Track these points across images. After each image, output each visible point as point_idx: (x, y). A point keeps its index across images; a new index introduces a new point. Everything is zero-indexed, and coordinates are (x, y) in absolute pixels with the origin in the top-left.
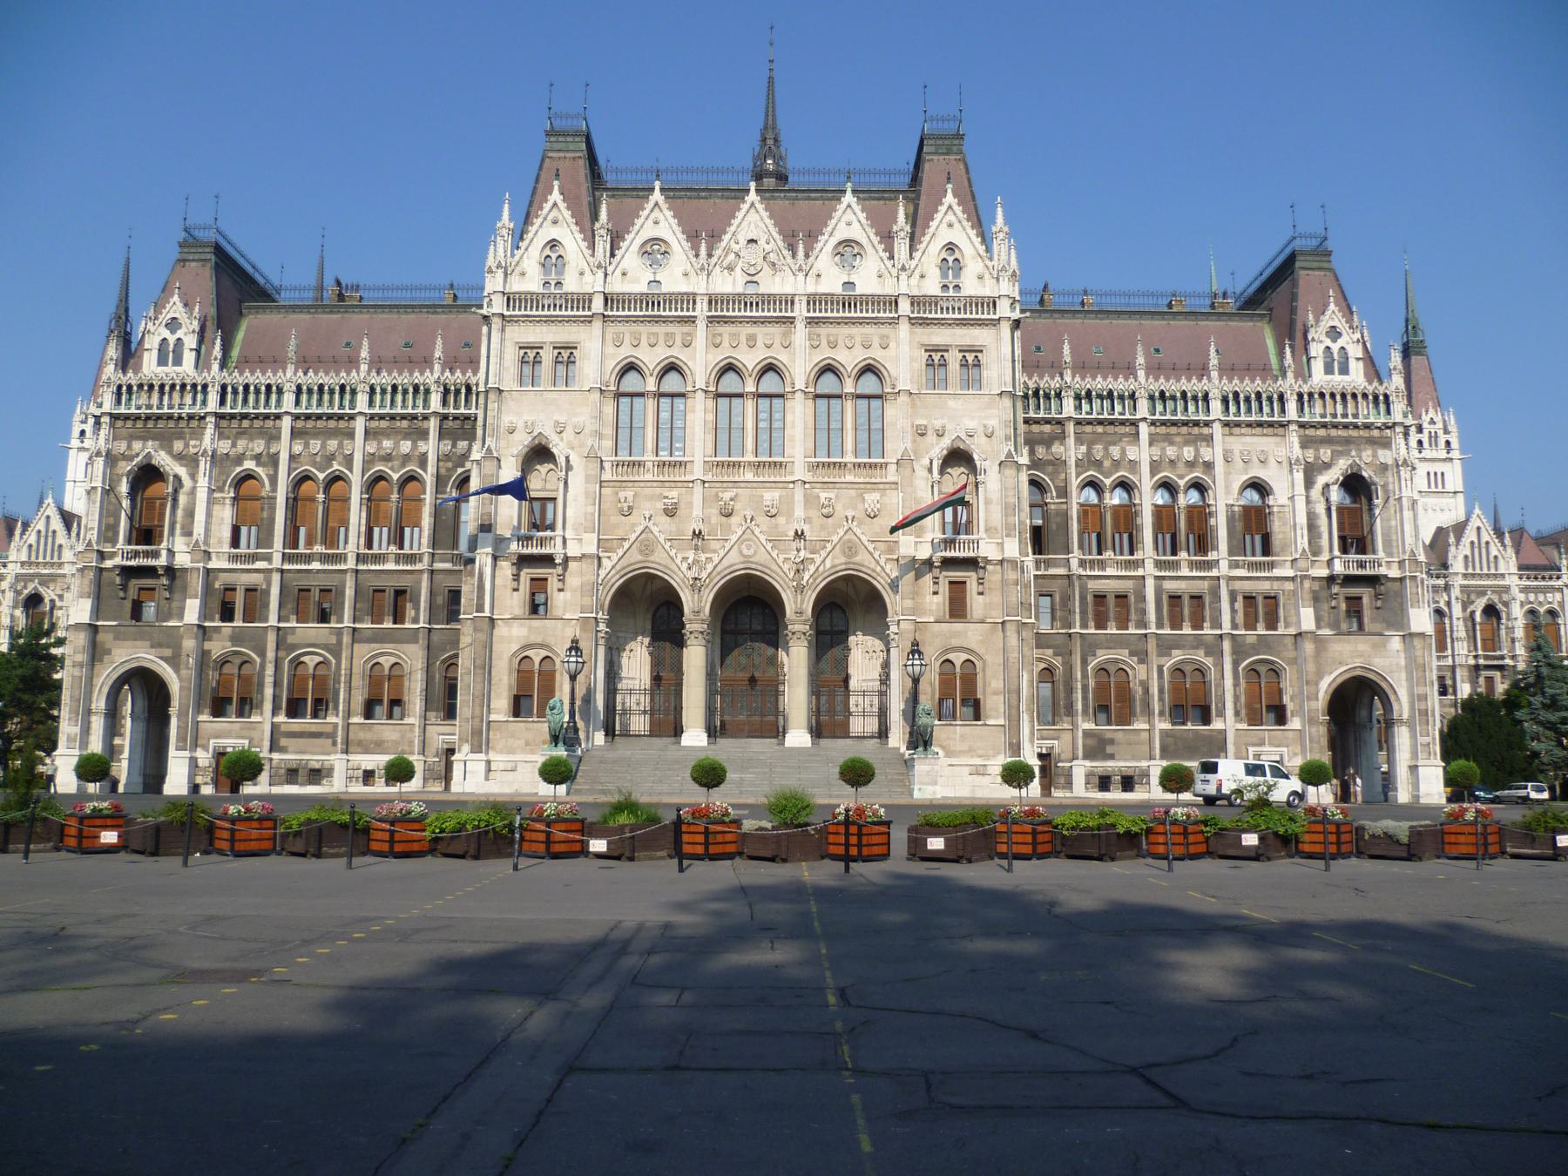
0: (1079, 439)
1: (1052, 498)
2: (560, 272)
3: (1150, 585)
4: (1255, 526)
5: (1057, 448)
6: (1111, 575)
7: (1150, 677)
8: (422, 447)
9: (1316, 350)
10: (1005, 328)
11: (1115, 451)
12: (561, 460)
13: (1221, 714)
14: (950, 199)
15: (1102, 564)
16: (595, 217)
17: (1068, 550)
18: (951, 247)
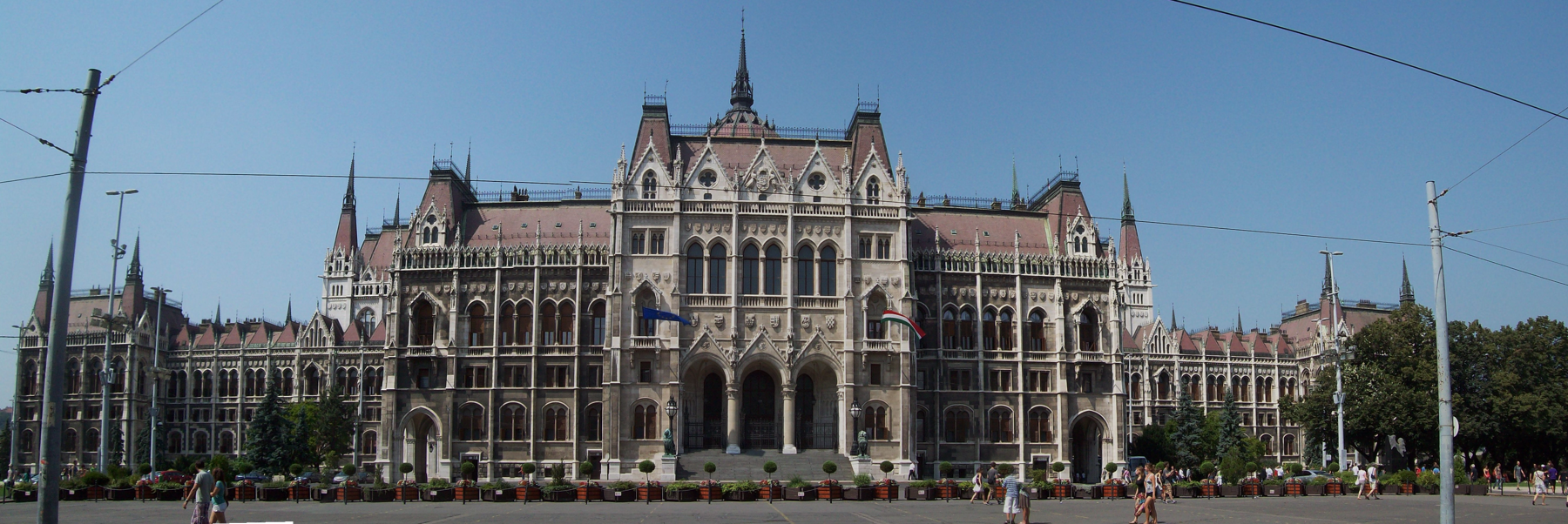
0: (944, 285)
1: (929, 318)
2: (654, 188)
3: (981, 365)
4: (1035, 332)
5: (931, 289)
6: (960, 360)
7: (980, 416)
8: (572, 286)
9: (1069, 238)
10: (903, 227)
11: (963, 290)
12: (658, 296)
13: (1017, 436)
14: (873, 151)
15: (955, 354)
16: (674, 156)
17: (937, 346)
18: (873, 179)
